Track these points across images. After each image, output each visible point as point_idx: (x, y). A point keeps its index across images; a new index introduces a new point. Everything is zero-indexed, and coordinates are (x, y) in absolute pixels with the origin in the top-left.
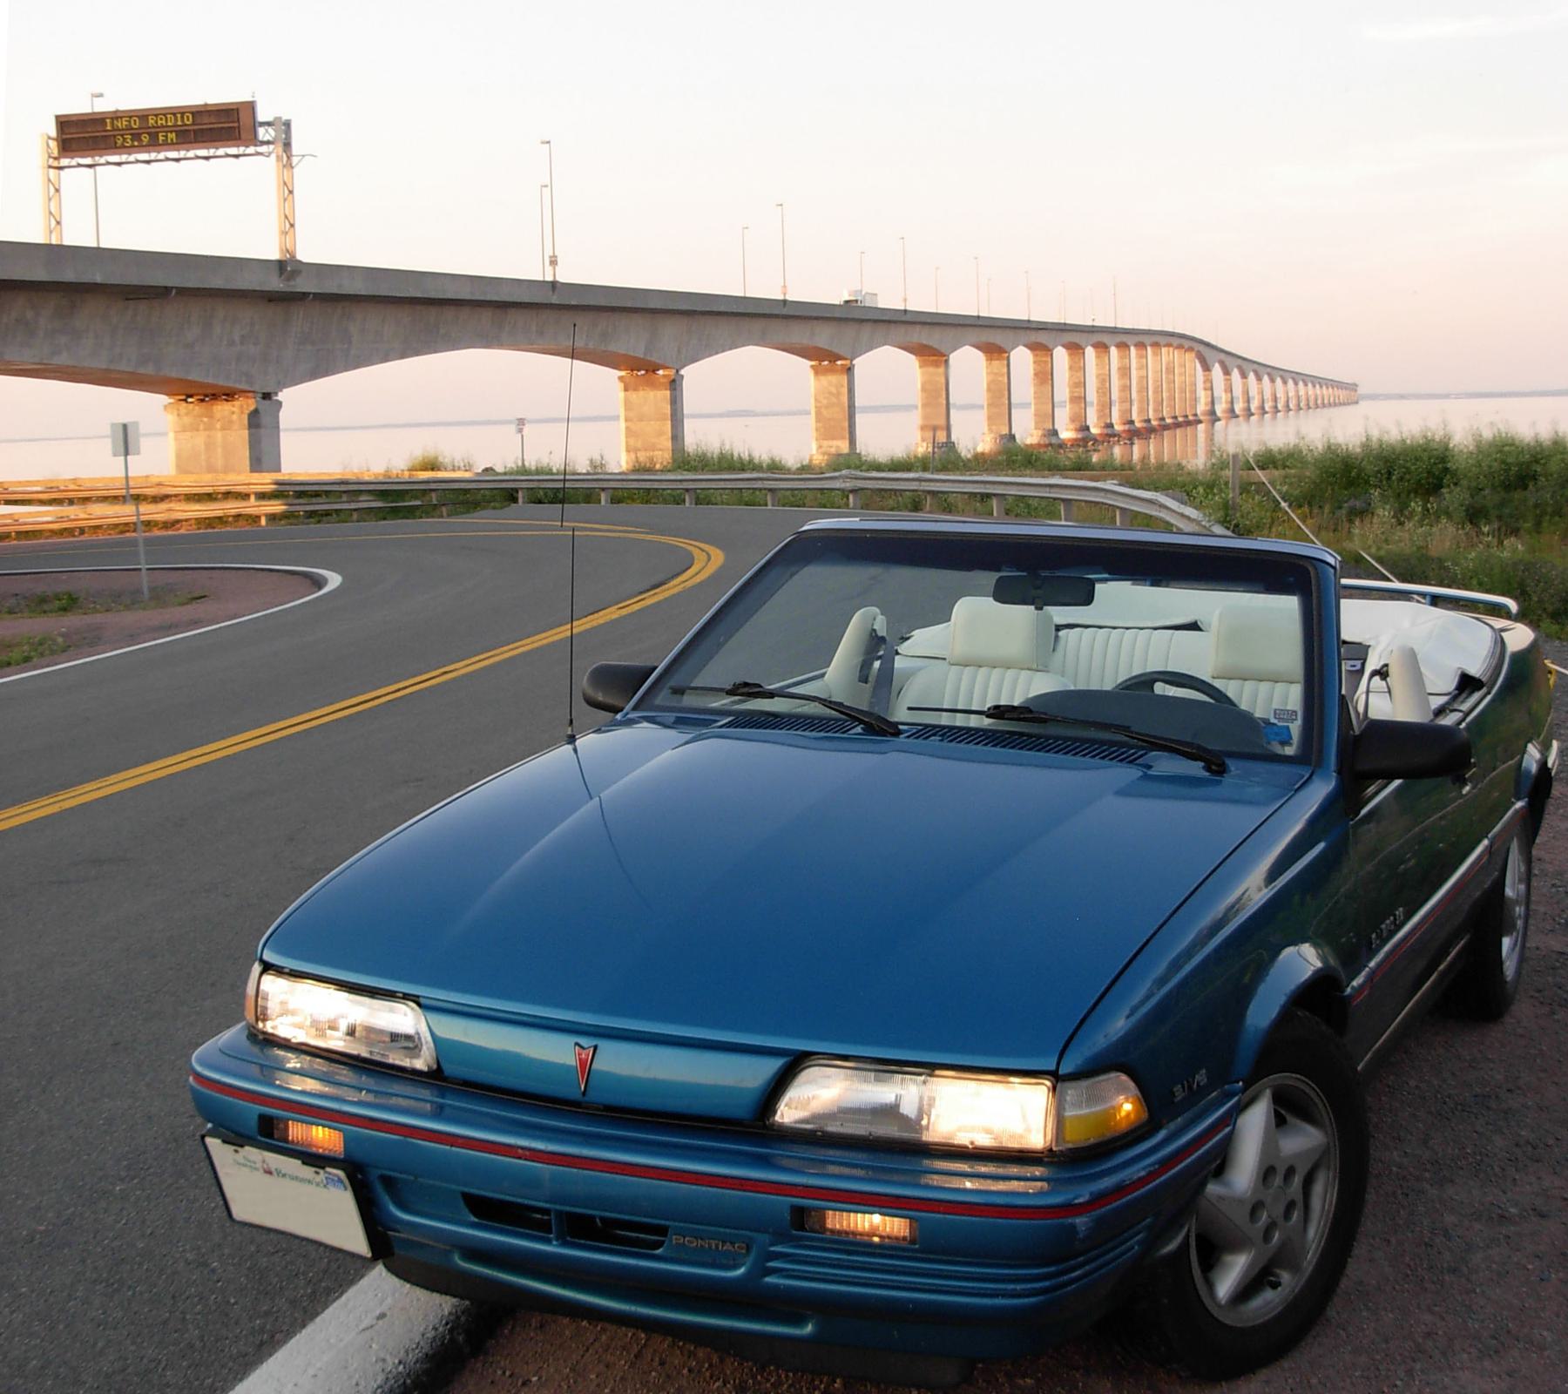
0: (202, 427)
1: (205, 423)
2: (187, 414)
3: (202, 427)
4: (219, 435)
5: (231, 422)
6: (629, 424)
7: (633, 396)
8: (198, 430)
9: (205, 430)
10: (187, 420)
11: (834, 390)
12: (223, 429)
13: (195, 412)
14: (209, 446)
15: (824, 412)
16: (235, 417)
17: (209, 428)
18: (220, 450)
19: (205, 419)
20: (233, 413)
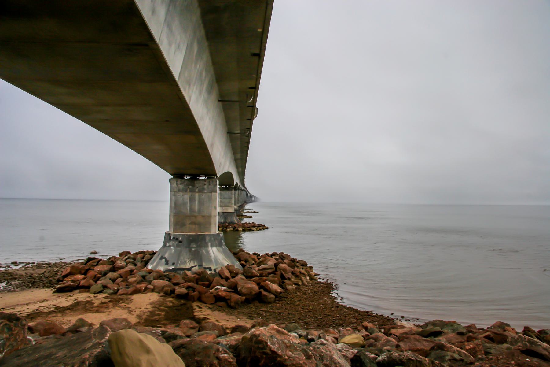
0: (188, 190)
1: (190, 189)
2: (181, 184)
3: (188, 190)
4: (197, 194)
5: (204, 189)
6: (221, 200)
7: (223, 192)
8: (186, 191)
9: (190, 191)
10: (181, 187)
12: (199, 191)
13: (185, 184)
14: (192, 200)
16: (206, 187)
17: (192, 191)
18: (197, 202)
19: (190, 187)
20: (205, 184)
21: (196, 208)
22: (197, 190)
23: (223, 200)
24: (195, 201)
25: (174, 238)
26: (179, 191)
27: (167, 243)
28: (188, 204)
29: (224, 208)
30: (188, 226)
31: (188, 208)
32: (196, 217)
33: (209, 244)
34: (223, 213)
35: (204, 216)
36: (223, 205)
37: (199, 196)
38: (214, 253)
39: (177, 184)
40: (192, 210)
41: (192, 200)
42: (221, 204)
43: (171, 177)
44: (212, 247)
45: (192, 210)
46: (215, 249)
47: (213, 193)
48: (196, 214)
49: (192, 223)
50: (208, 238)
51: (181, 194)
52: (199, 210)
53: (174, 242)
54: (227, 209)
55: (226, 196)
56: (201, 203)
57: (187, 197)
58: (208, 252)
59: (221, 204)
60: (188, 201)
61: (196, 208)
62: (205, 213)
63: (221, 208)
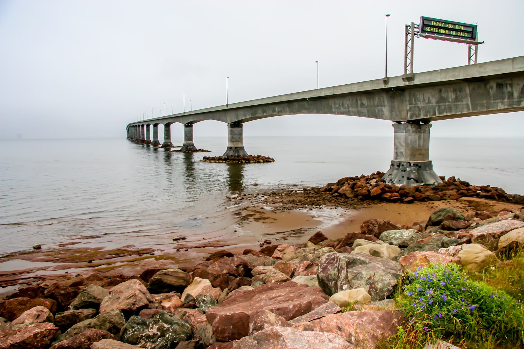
0: (418, 132)
3: (418, 132)
4: (422, 134)
5: (426, 131)
8: (416, 132)
10: (414, 129)
11: (189, 130)
12: (424, 133)
14: (419, 138)
15: (188, 135)
17: (420, 132)
19: (419, 129)
20: (426, 128)
21: (422, 144)
22: (422, 132)
23: (234, 136)
24: (421, 139)
25: (414, 165)
26: (413, 132)
27: (407, 169)
28: (418, 142)
29: (235, 143)
30: (417, 156)
31: (418, 144)
32: (421, 150)
34: (236, 148)
35: (425, 149)
36: (235, 140)
37: (423, 135)
39: (412, 127)
40: (419, 145)
42: (233, 140)
45: (419, 145)
48: (421, 148)
49: (420, 154)
51: (414, 134)
52: (423, 145)
53: (415, 168)
54: (238, 144)
55: (237, 132)
57: (417, 136)
59: (233, 140)
60: (417, 139)
61: (422, 144)
62: (426, 148)
63: (233, 143)
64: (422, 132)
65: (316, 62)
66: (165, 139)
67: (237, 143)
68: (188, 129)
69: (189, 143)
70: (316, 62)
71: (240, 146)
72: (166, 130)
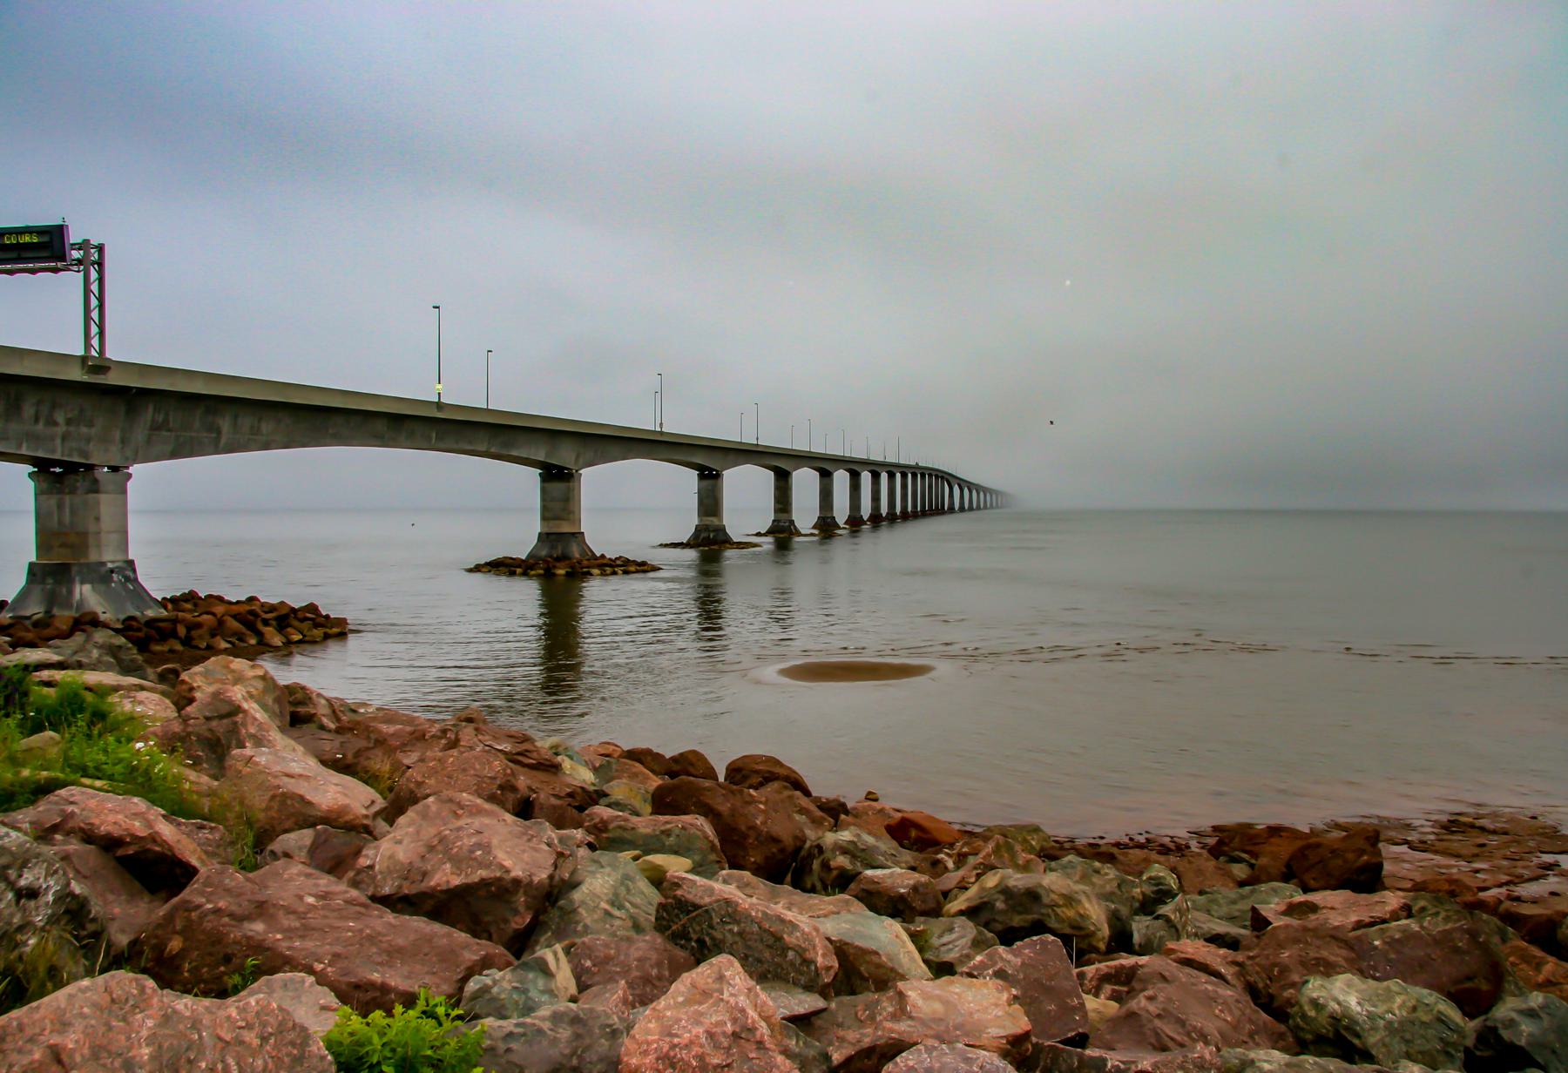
4: (67, 498)
8: (52, 493)
14: (60, 506)
17: (61, 492)
18: (67, 510)
20: (78, 481)
29: (552, 523)
33: (77, 579)
35: (78, 534)
38: (81, 594)
41: (60, 506)
43: (31, 469)
44: (82, 583)
45: (60, 522)
46: (87, 588)
47: (91, 496)
49: (63, 545)
50: (74, 569)
56: (73, 512)
58: (71, 592)
59: (547, 515)
64: (67, 490)
65: (434, 307)
66: (775, 512)
67: (557, 522)
68: (706, 483)
69: (707, 523)
70: (434, 307)
71: (566, 528)
72: (777, 488)
